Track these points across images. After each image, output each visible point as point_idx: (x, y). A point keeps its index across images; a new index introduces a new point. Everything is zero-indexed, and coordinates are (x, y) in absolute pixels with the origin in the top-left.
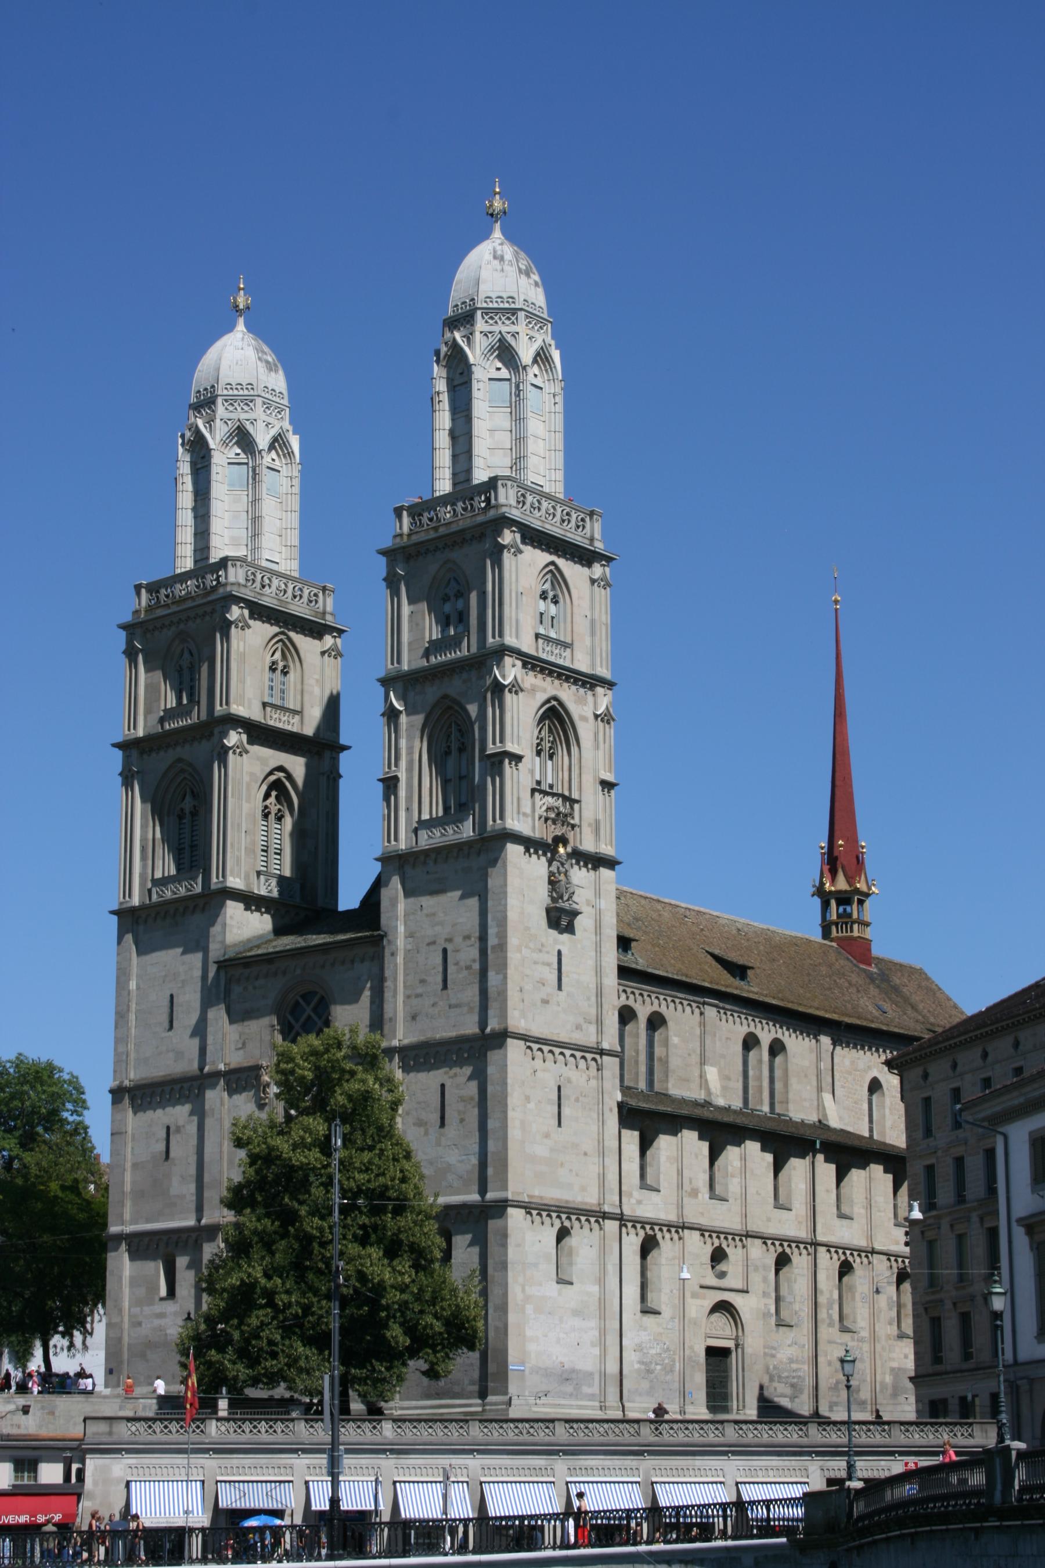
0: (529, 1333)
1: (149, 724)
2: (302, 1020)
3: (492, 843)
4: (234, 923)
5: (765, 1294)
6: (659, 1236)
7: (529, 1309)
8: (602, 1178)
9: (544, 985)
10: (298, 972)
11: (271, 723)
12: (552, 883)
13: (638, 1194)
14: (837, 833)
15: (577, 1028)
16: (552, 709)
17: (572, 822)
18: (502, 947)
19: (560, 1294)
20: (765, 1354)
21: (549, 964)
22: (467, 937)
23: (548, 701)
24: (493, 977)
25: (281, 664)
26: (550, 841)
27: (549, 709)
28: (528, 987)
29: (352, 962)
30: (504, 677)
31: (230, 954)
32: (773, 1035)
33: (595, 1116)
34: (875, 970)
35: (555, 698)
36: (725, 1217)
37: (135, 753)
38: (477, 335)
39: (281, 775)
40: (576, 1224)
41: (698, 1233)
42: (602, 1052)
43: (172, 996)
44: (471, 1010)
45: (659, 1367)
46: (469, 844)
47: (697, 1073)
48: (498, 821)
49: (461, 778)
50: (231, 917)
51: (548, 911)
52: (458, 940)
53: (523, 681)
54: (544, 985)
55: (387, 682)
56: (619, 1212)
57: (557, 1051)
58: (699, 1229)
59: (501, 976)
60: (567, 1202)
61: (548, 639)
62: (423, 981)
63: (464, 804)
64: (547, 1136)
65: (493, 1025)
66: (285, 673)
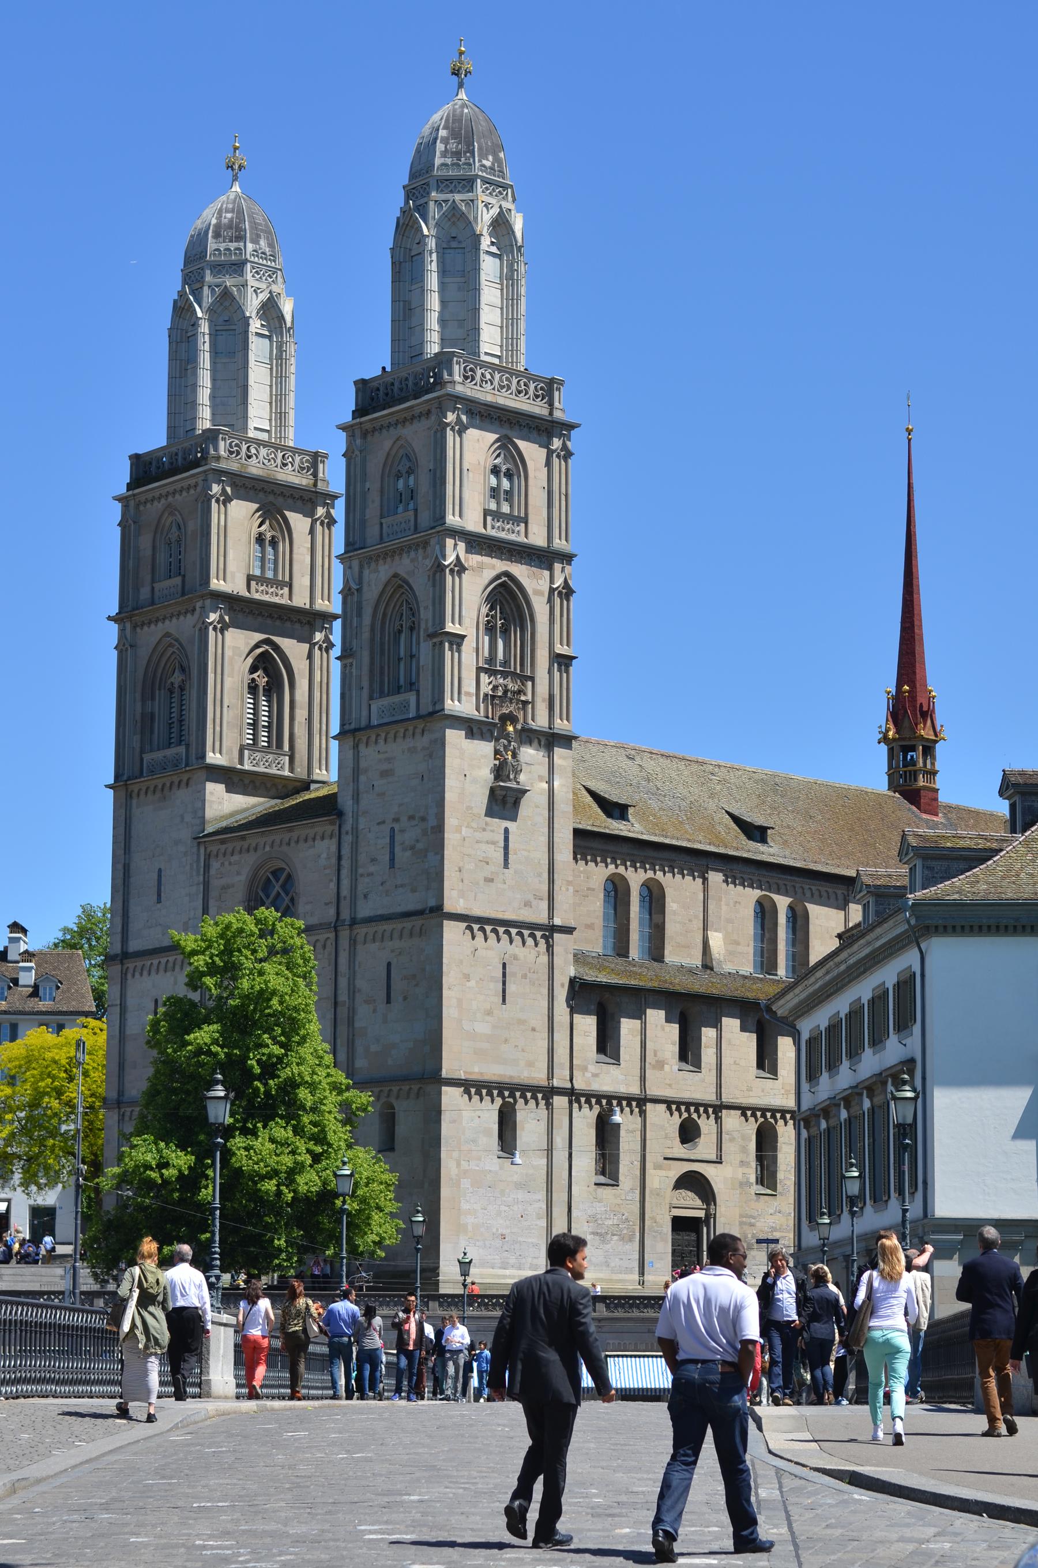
0: (465, 1206)
1: (142, 597)
2: (272, 896)
4: (213, 799)
7: (465, 1183)
9: (487, 863)
10: (267, 849)
11: (257, 596)
13: (592, 1068)
15: (525, 905)
17: (523, 698)
18: (439, 829)
19: (501, 1168)
20: (741, 1223)
21: (494, 843)
22: (411, 818)
23: (498, 577)
25: (269, 535)
27: (500, 585)
29: (314, 839)
30: (444, 558)
31: (209, 829)
34: (943, 820)
35: (506, 574)
36: (697, 1087)
37: (128, 625)
38: (432, 204)
40: (521, 1101)
41: (663, 1106)
43: (160, 870)
45: (615, 1238)
49: (412, 656)
50: (211, 793)
51: (492, 790)
52: (404, 818)
53: (466, 559)
54: (487, 863)
56: (569, 1086)
60: (511, 1077)
61: (497, 515)
62: (373, 860)
64: (489, 1013)
66: (274, 543)
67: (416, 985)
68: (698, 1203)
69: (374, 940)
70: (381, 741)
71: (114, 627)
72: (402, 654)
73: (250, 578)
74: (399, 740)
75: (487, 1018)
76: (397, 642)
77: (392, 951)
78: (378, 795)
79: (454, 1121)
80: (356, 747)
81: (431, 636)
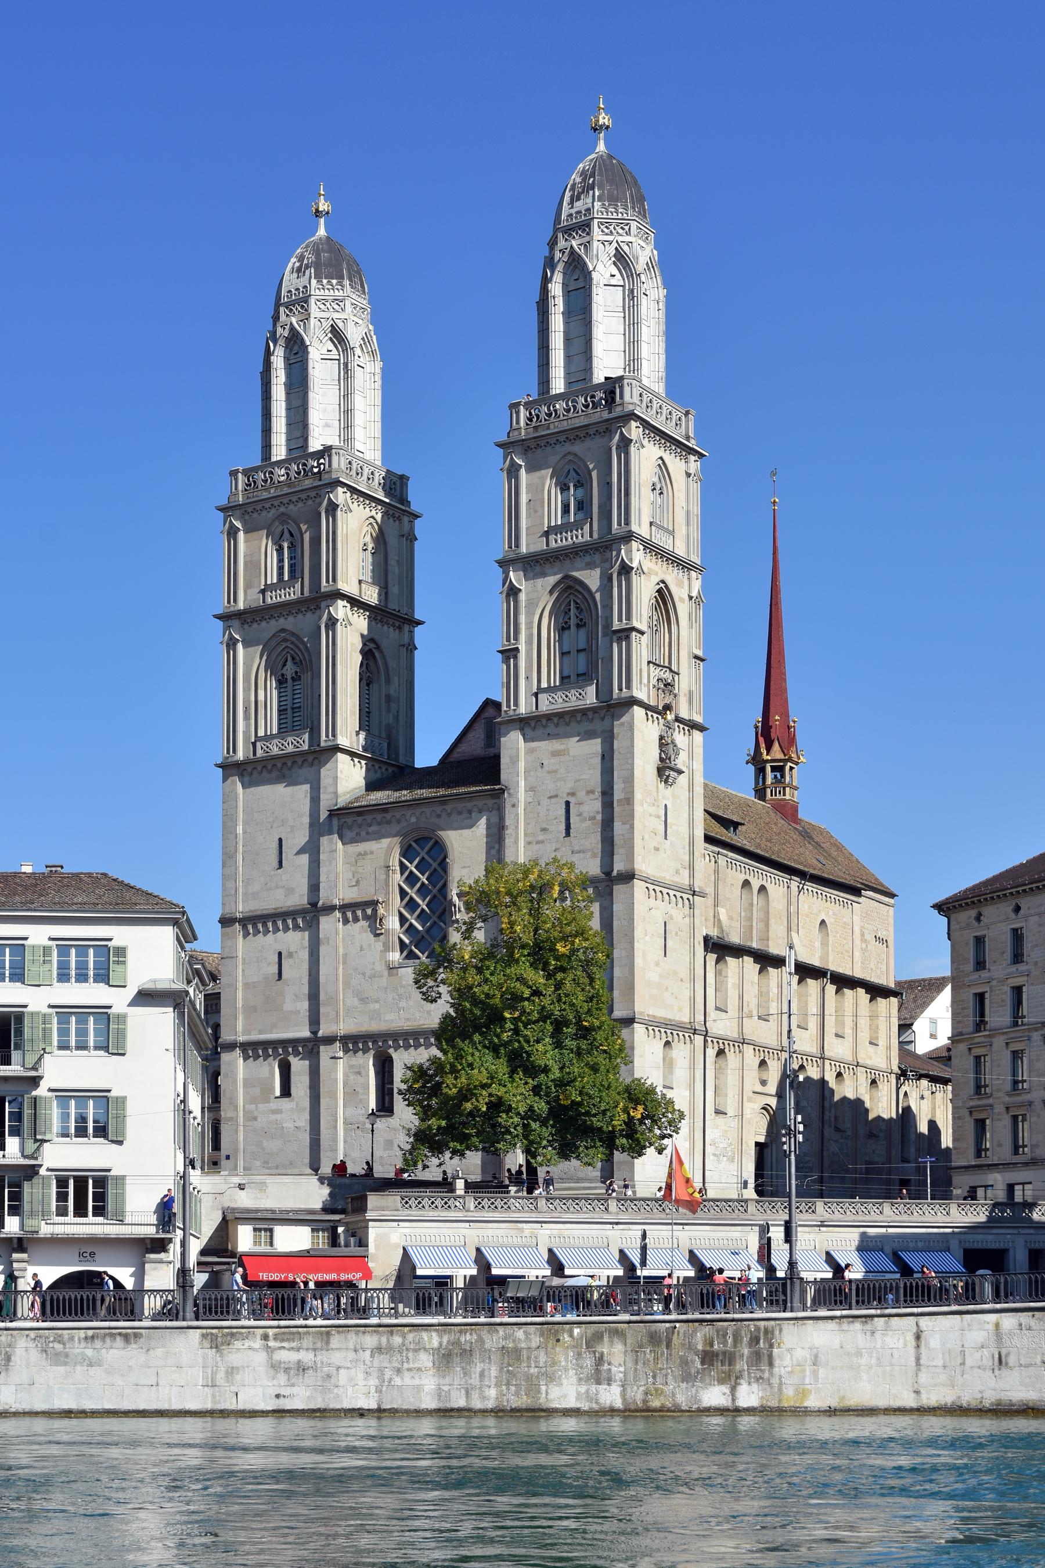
3: (614, 708)
14: (772, 710)
18: (629, 801)
21: (658, 817)
22: (591, 792)
24: (618, 827)
26: (660, 708)
28: (646, 837)
29: (470, 812)
32: (760, 882)
44: (594, 856)
46: (594, 710)
47: (712, 914)
48: (624, 690)
51: (660, 771)
52: (581, 794)
55: (504, 564)
59: (628, 826)
62: (544, 830)
63: (584, 674)
64: (657, 964)
65: (618, 866)
70: (551, 725)
74: (574, 724)
78: (549, 772)
80: (522, 730)
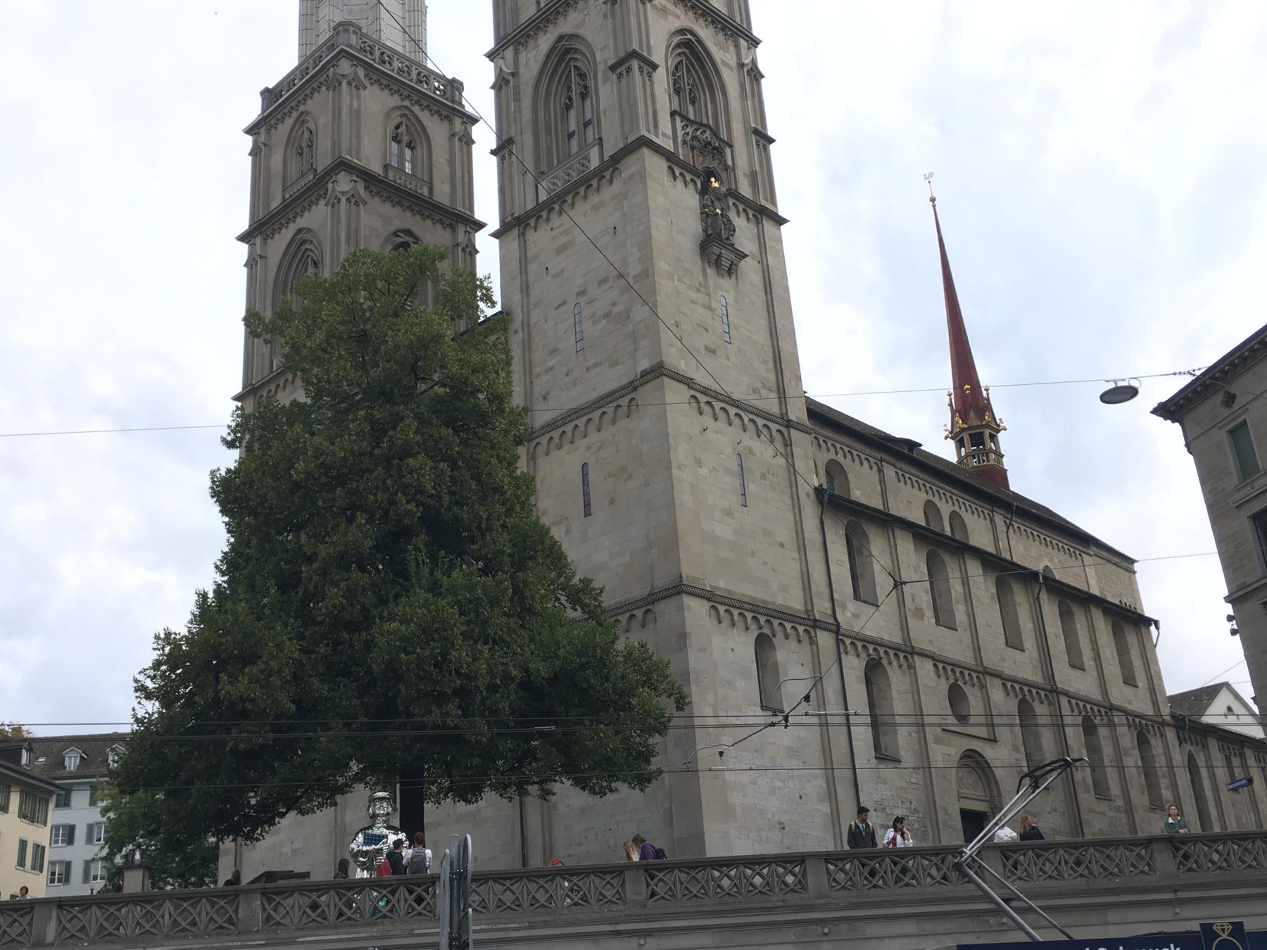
5: (1015, 748)
6: (885, 662)
8: (806, 577)
12: (706, 215)
13: (852, 606)
16: (686, 44)
22: (605, 280)
25: (405, 139)
33: (789, 501)
37: (258, 240)
39: (410, 240)
40: (780, 634)
42: (789, 424)
44: (614, 364)
46: (599, 173)
49: (587, 124)
57: (732, 411)
58: (933, 658)
60: (764, 601)
64: (729, 513)
67: (629, 478)
68: (980, 793)
69: (560, 447)
70: (554, 216)
71: (244, 248)
72: (573, 127)
73: (386, 167)
75: (728, 520)
76: (565, 119)
77: (588, 449)
79: (702, 650)
81: (613, 68)
